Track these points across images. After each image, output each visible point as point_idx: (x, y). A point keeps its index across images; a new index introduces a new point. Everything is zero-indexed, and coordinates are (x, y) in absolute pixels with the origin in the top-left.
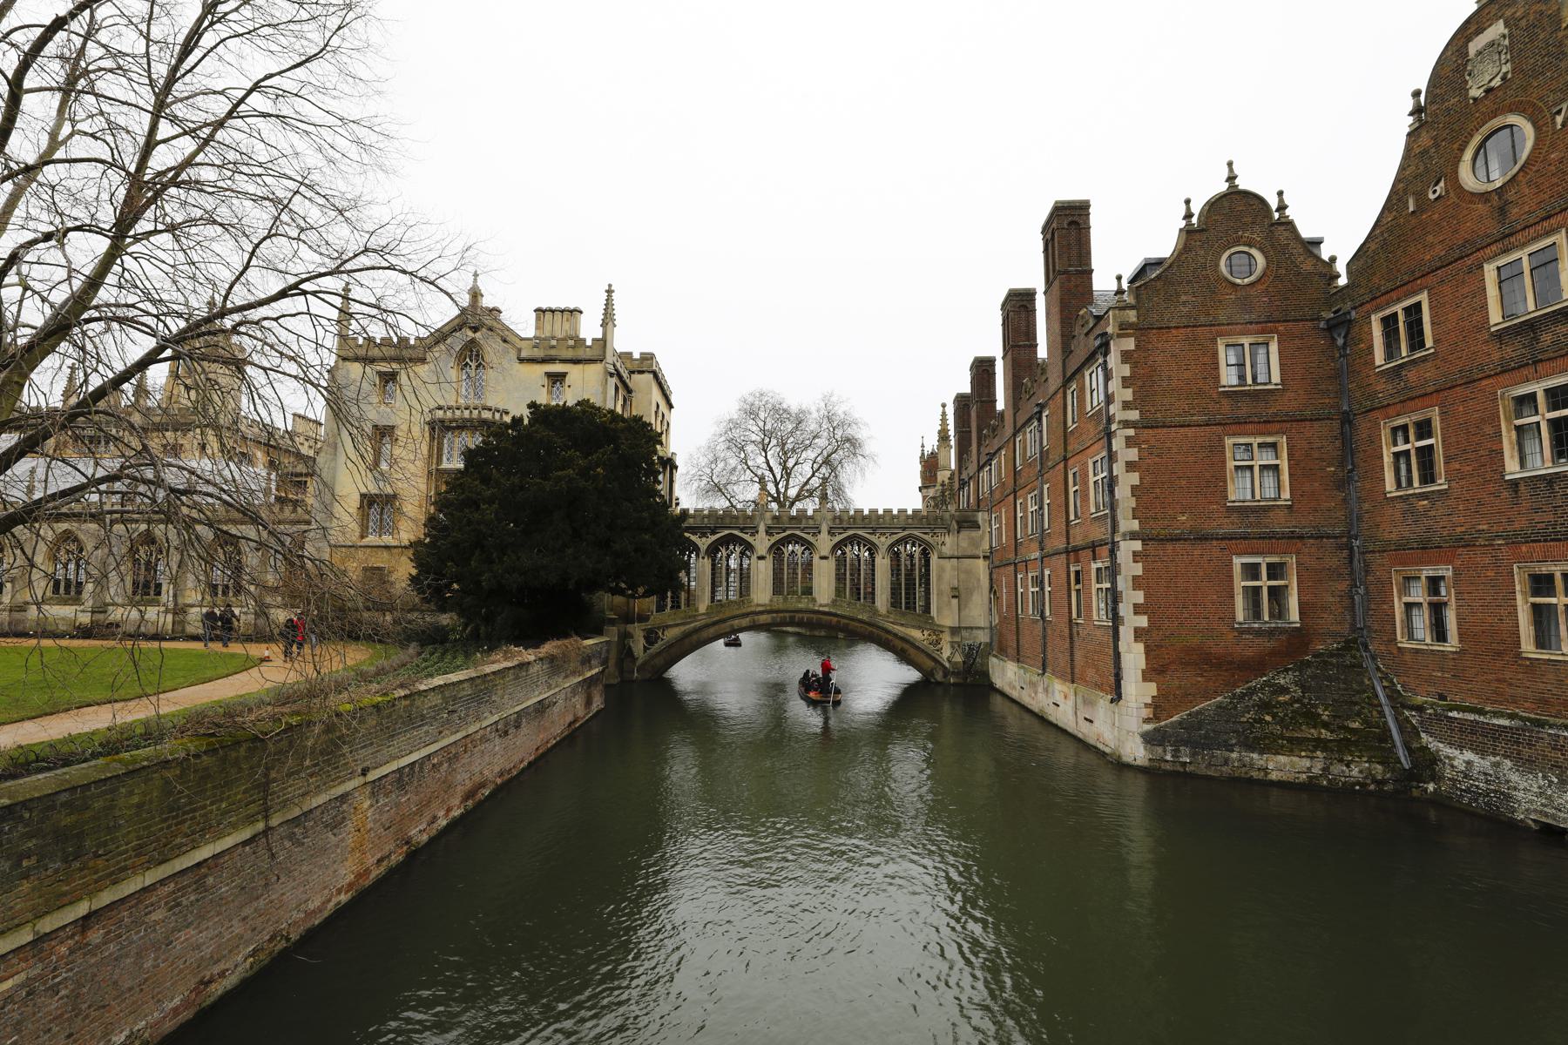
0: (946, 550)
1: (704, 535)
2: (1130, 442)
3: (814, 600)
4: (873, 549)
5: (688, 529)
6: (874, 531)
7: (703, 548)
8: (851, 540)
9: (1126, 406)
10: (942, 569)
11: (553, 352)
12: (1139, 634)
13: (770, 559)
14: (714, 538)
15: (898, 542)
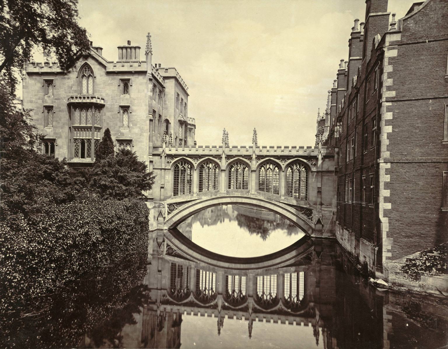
2: (389, 110)
7: (195, 165)
12: (387, 213)
13: (227, 172)
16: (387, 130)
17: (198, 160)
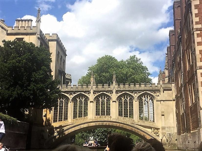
0: (159, 98)
1: (71, 94)
3: (111, 117)
4: (132, 98)
5: (65, 92)
6: (132, 91)
8: (123, 95)
9: (197, 23)
10: (158, 106)
11: (19, 31)
14: (75, 95)
15: (142, 95)
16: (198, 48)
17: (72, 95)
